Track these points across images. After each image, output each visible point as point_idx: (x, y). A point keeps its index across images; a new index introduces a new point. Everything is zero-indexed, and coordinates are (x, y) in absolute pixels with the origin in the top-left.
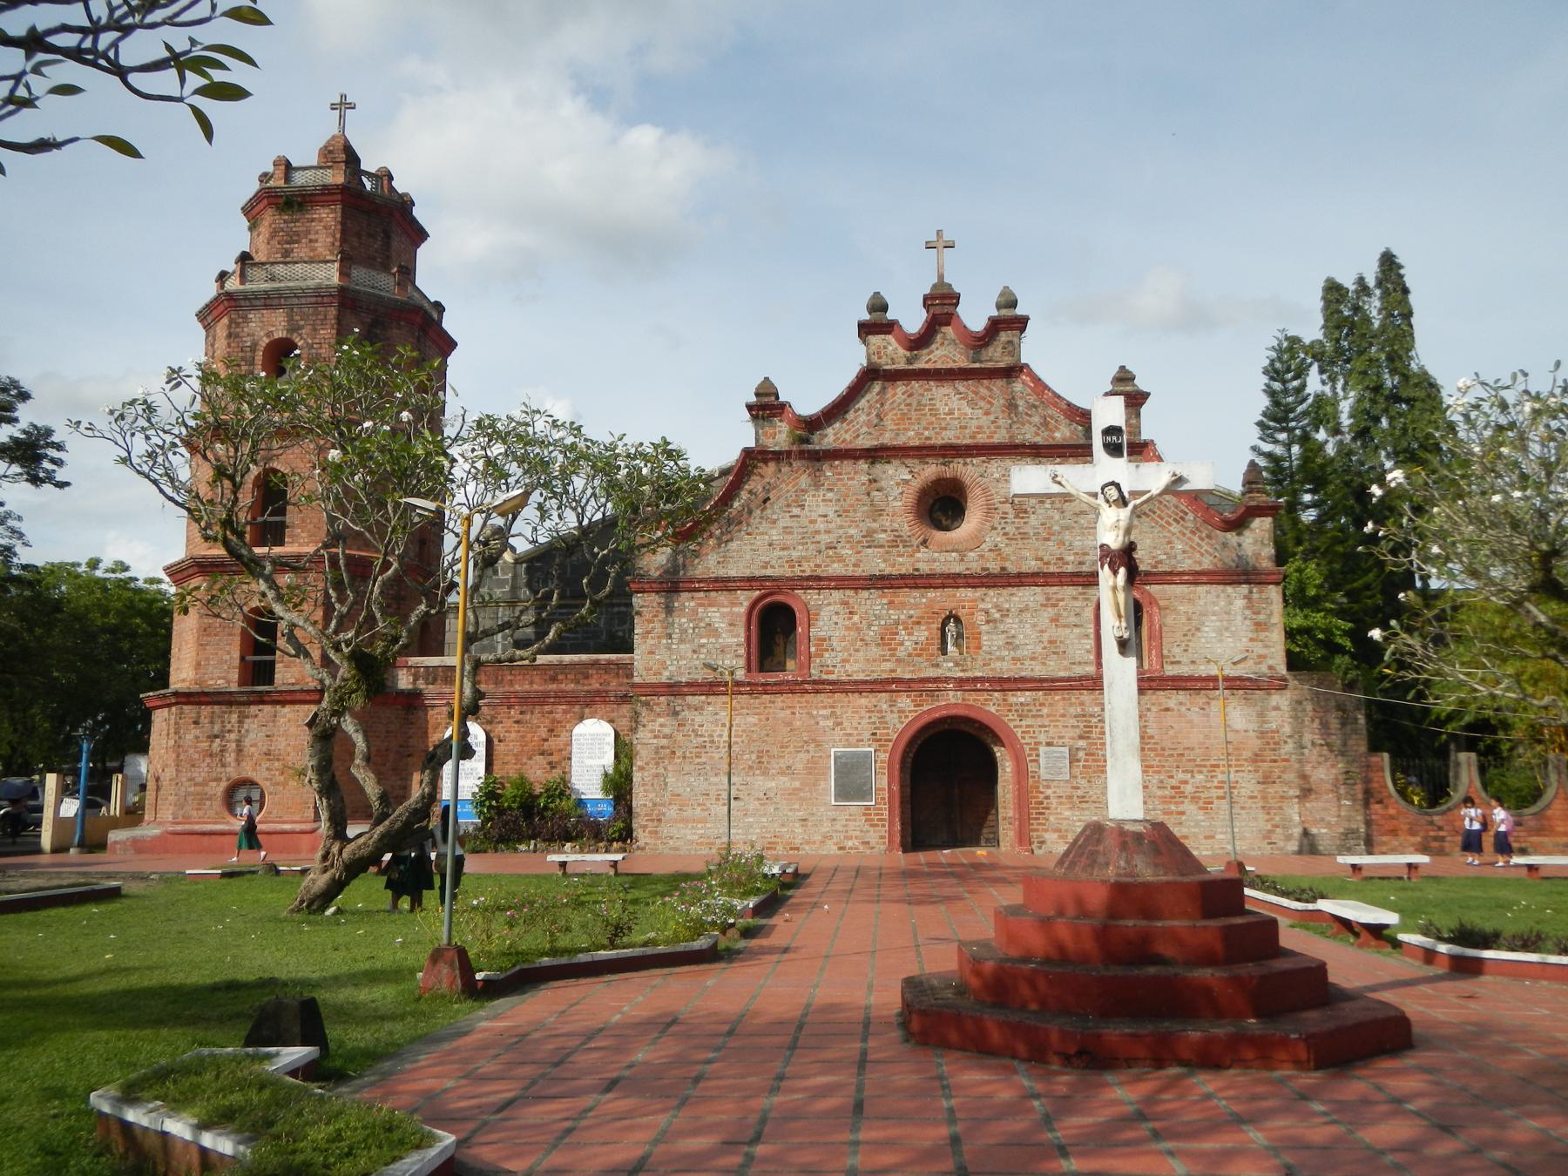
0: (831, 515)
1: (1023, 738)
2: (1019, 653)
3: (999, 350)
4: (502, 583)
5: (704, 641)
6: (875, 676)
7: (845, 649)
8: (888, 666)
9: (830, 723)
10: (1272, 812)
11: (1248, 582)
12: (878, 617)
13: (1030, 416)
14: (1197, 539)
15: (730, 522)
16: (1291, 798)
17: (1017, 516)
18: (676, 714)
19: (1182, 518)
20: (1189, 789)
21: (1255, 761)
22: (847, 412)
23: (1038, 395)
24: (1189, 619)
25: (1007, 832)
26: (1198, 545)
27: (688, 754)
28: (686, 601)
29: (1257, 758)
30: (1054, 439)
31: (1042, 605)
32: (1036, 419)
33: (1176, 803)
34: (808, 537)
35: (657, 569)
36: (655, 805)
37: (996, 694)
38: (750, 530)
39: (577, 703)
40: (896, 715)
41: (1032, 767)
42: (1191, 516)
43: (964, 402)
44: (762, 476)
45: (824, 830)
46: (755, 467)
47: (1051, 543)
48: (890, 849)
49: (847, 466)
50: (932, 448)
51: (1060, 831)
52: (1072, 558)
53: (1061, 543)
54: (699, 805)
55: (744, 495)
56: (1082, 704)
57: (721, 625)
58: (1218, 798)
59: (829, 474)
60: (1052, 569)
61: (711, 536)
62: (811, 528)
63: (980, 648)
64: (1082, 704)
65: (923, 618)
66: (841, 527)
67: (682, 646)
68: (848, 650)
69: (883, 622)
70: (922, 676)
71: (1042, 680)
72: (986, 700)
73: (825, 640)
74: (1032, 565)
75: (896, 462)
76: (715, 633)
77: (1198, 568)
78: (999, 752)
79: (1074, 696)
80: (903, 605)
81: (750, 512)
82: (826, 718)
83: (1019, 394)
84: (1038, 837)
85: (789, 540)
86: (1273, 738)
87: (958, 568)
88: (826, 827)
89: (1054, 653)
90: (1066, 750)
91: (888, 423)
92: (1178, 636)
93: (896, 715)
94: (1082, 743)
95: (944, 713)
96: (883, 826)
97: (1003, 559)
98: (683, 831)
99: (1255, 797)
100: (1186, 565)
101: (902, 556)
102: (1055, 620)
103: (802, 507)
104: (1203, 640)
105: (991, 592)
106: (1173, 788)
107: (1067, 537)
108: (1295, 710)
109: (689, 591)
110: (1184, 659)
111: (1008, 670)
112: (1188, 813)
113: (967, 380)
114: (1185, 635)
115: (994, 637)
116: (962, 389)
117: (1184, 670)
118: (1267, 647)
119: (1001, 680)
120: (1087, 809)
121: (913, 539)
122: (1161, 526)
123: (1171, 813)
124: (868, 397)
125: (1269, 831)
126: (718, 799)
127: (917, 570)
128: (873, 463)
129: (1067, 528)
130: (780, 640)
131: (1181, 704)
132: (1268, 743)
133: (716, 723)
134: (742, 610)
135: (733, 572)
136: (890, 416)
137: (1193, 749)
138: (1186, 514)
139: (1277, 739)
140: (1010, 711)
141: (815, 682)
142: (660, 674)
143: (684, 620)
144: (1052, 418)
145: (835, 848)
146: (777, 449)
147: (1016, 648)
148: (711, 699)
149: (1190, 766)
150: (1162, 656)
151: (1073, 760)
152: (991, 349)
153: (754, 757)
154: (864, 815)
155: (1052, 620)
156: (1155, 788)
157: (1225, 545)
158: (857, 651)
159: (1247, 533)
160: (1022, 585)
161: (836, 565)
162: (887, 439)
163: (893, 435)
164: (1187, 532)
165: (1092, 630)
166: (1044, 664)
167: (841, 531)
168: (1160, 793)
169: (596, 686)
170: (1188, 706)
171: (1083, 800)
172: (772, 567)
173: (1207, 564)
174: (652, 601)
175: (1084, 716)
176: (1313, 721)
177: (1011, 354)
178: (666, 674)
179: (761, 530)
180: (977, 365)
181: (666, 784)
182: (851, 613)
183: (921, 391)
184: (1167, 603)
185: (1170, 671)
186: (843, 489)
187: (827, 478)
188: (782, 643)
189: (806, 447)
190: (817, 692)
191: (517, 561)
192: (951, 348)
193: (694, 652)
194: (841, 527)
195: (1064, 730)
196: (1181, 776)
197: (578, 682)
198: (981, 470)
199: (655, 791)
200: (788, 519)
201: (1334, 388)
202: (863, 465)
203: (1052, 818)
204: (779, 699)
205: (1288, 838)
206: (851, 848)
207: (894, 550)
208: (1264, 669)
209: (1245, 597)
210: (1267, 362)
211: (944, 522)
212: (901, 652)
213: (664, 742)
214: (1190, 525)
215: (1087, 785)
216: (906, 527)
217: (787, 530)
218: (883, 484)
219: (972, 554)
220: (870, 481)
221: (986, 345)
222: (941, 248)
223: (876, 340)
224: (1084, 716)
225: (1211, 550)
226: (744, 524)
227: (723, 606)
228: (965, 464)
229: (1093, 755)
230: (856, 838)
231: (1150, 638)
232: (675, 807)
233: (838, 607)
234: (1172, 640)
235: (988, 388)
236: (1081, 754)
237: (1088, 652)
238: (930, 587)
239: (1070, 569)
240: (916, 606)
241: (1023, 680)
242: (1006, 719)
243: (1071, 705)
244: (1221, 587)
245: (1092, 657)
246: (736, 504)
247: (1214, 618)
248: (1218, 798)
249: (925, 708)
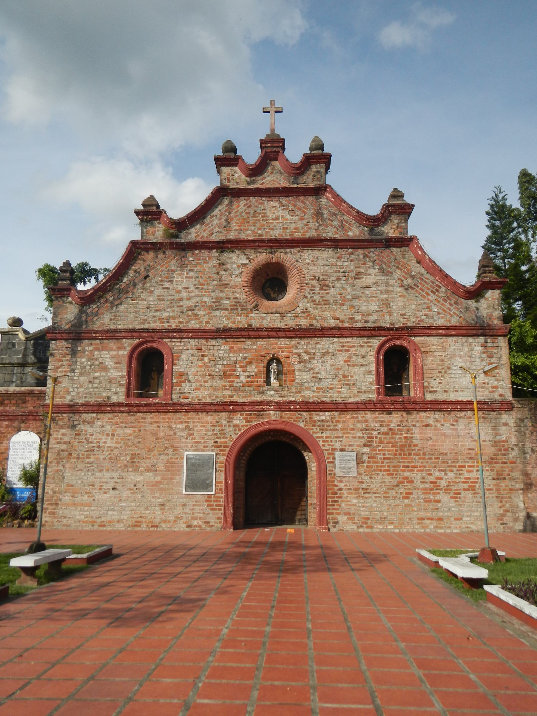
0: (192, 287)
1: (324, 445)
2: (321, 385)
3: (311, 177)
4: (19, 352)
5: (97, 374)
6: (218, 400)
7: (197, 381)
8: (227, 393)
9: (184, 434)
10: (504, 500)
11: (485, 336)
12: (221, 359)
13: (332, 221)
14: (447, 305)
15: (120, 291)
16: (518, 490)
17: (321, 289)
18: (74, 426)
19: (437, 290)
20: (443, 483)
21: (490, 463)
22: (205, 218)
23: (337, 206)
24: (442, 361)
25: (313, 515)
26: (449, 309)
27: (81, 456)
28: (86, 347)
29: (492, 461)
30: (348, 236)
31: (339, 351)
32: (336, 223)
33: (434, 494)
34: (175, 302)
35: (67, 324)
36: (54, 493)
37: (304, 414)
38: (134, 297)
39: (16, 420)
40: (232, 429)
41: (329, 467)
42: (443, 289)
43: (286, 212)
44: (144, 261)
45: (177, 512)
46: (140, 254)
47: (345, 308)
48: (224, 527)
49: (204, 254)
50: (262, 241)
51: (349, 514)
52: (360, 318)
53: (353, 307)
54: (86, 493)
55: (131, 273)
56: (366, 421)
57: (110, 363)
58: (465, 490)
59: (191, 259)
60: (346, 325)
61: (106, 301)
62: (177, 296)
63: (294, 381)
64: (366, 421)
65: (254, 359)
66: (198, 296)
67: (81, 378)
68: (200, 382)
69: (225, 362)
70: (252, 400)
71: (337, 404)
72: (297, 418)
73: (183, 374)
74: (332, 323)
75: (238, 252)
76: (106, 369)
77: (448, 325)
78: (307, 456)
79: (361, 416)
80: (240, 350)
81: (135, 285)
82: (182, 430)
83: (324, 206)
84: (333, 518)
85: (161, 304)
86: (503, 446)
87: (280, 324)
88: (178, 511)
89: (347, 384)
90: (354, 454)
91: (234, 225)
92: (435, 373)
93: (232, 429)
94: (366, 450)
95: (267, 427)
96: (220, 510)
97: (312, 318)
98: (73, 513)
99: (492, 490)
100: (441, 322)
101: (240, 316)
102: (347, 361)
103: (171, 282)
104: (453, 376)
105: (303, 342)
106: (431, 482)
107: (356, 303)
108: (518, 426)
109: (89, 339)
110: (439, 389)
111: (313, 397)
112: (443, 501)
113: (288, 196)
114: (440, 372)
115: (304, 373)
116: (285, 203)
117: (440, 397)
118: (497, 380)
119: (308, 403)
120: (369, 498)
121: (248, 304)
122: (423, 296)
123: (430, 501)
124: (220, 207)
125: (503, 515)
126: (100, 489)
127: (251, 325)
128: (222, 252)
129: (357, 297)
130: (155, 375)
131: (437, 421)
132: (500, 450)
133: (102, 433)
134: (125, 353)
135: (120, 326)
136: (234, 221)
137: (446, 454)
138: (440, 287)
139: (506, 447)
140: (314, 426)
141: (174, 404)
142: (65, 398)
143: (84, 360)
144: (347, 222)
145: (184, 526)
146: (154, 241)
147: (320, 381)
148: (100, 416)
149: (444, 466)
150: (424, 387)
151: (359, 462)
152: (305, 177)
153: (128, 458)
154: (207, 501)
155: (345, 361)
156: (419, 482)
157: (467, 309)
158: (206, 382)
159: (483, 301)
160: (323, 336)
161: (193, 322)
162: (232, 236)
163: (236, 233)
164: (441, 300)
165: (374, 369)
166: (339, 392)
167: (198, 299)
168: (422, 486)
169: (31, 408)
170: (442, 423)
171: (366, 491)
172: (149, 323)
173: (455, 321)
174: (62, 346)
175: (367, 430)
176: (532, 433)
177: (319, 179)
178: (69, 397)
179: (142, 297)
180: (295, 186)
181: (63, 478)
182: (203, 355)
183: (257, 204)
184: (426, 349)
185: (429, 397)
186: (200, 270)
187: (190, 262)
188: (156, 377)
189: (173, 240)
190: (176, 411)
191: (27, 340)
192: (278, 176)
193: (90, 382)
194: (198, 296)
195: (353, 440)
196: (437, 474)
197: (18, 406)
198: (297, 257)
199: (55, 482)
200: (161, 290)
201: (527, 237)
202: (215, 254)
203: (343, 505)
204: (149, 417)
205: (516, 520)
206: (196, 526)
207: (235, 312)
208: (496, 396)
209: (482, 345)
210: (488, 208)
211: (273, 296)
212: (237, 384)
213: (64, 447)
214: (443, 295)
215: (369, 480)
216: (244, 296)
217: (160, 298)
218: (228, 266)
219: (289, 315)
220: (219, 264)
221: (302, 173)
222: (273, 112)
223: (226, 170)
224: (367, 430)
225: (458, 313)
226: (130, 293)
227: (113, 350)
228: (286, 253)
229: (374, 458)
230: (200, 518)
231: (415, 374)
232: (69, 495)
233: (193, 351)
234: (431, 376)
235: (303, 202)
236: (365, 458)
237: (371, 384)
238: (259, 338)
239: (358, 325)
240: (249, 351)
241: (324, 403)
242: (311, 432)
243: (359, 422)
244: (465, 338)
245: (374, 387)
246: (125, 280)
247: (460, 360)
248: (465, 490)
249: (253, 424)
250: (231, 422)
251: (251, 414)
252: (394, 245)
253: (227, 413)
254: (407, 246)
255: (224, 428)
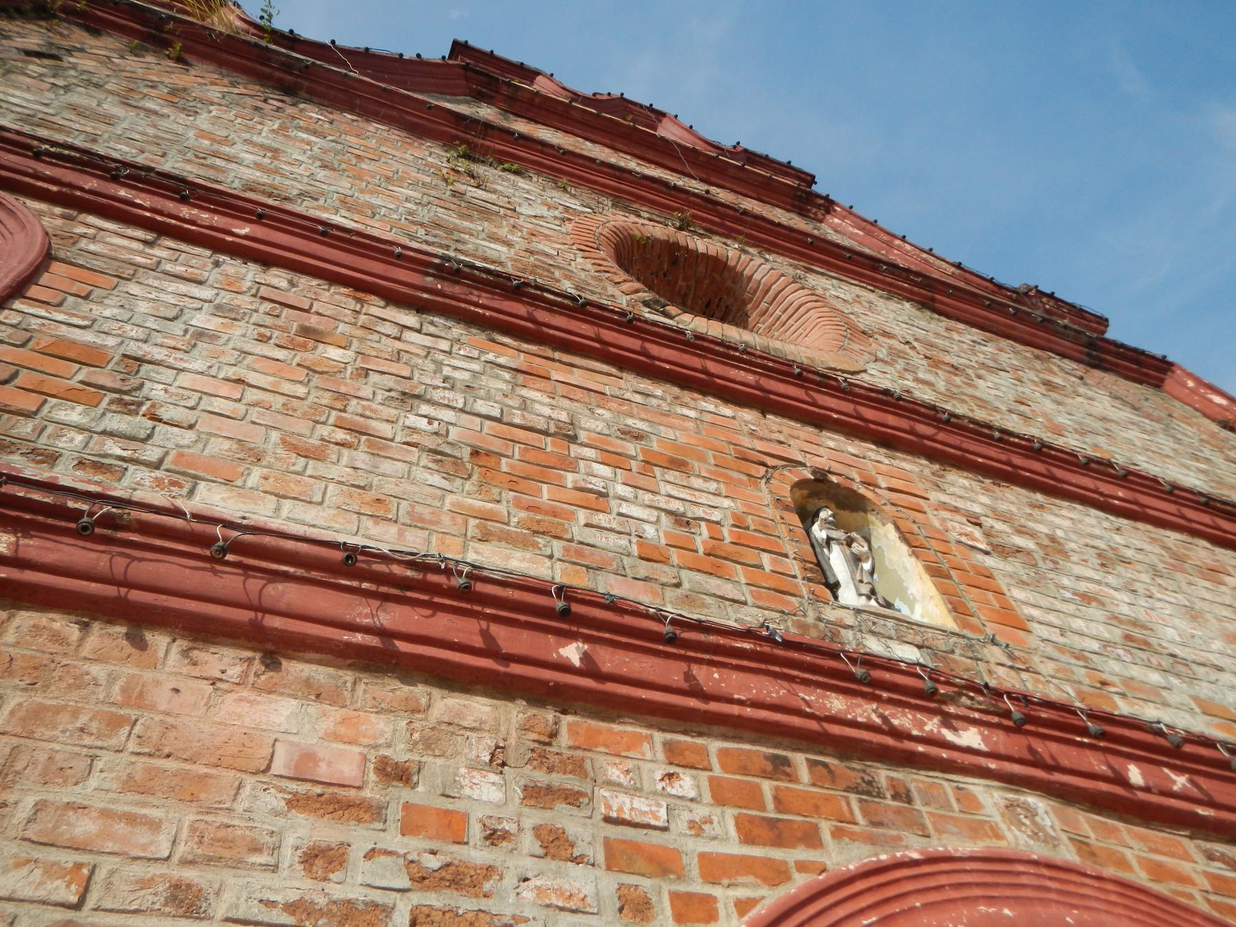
250: (573, 798)
251: (780, 768)
252: (1118, 365)
253: (515, 713)
254: (1158, 385)
255: (477, 854)
